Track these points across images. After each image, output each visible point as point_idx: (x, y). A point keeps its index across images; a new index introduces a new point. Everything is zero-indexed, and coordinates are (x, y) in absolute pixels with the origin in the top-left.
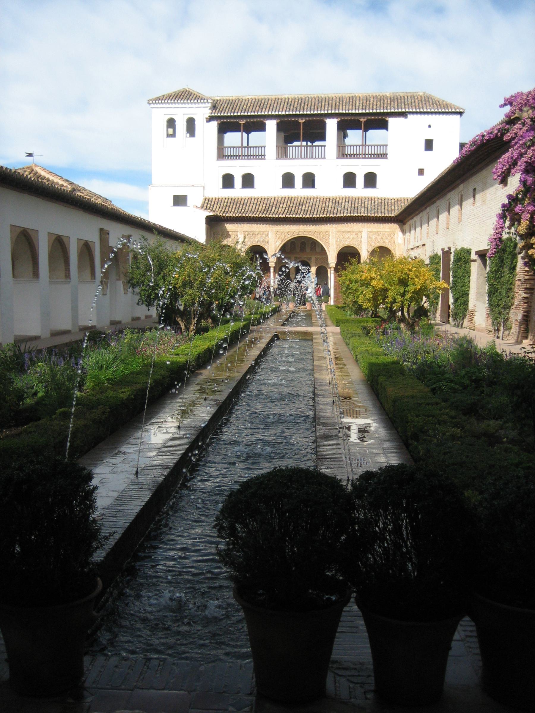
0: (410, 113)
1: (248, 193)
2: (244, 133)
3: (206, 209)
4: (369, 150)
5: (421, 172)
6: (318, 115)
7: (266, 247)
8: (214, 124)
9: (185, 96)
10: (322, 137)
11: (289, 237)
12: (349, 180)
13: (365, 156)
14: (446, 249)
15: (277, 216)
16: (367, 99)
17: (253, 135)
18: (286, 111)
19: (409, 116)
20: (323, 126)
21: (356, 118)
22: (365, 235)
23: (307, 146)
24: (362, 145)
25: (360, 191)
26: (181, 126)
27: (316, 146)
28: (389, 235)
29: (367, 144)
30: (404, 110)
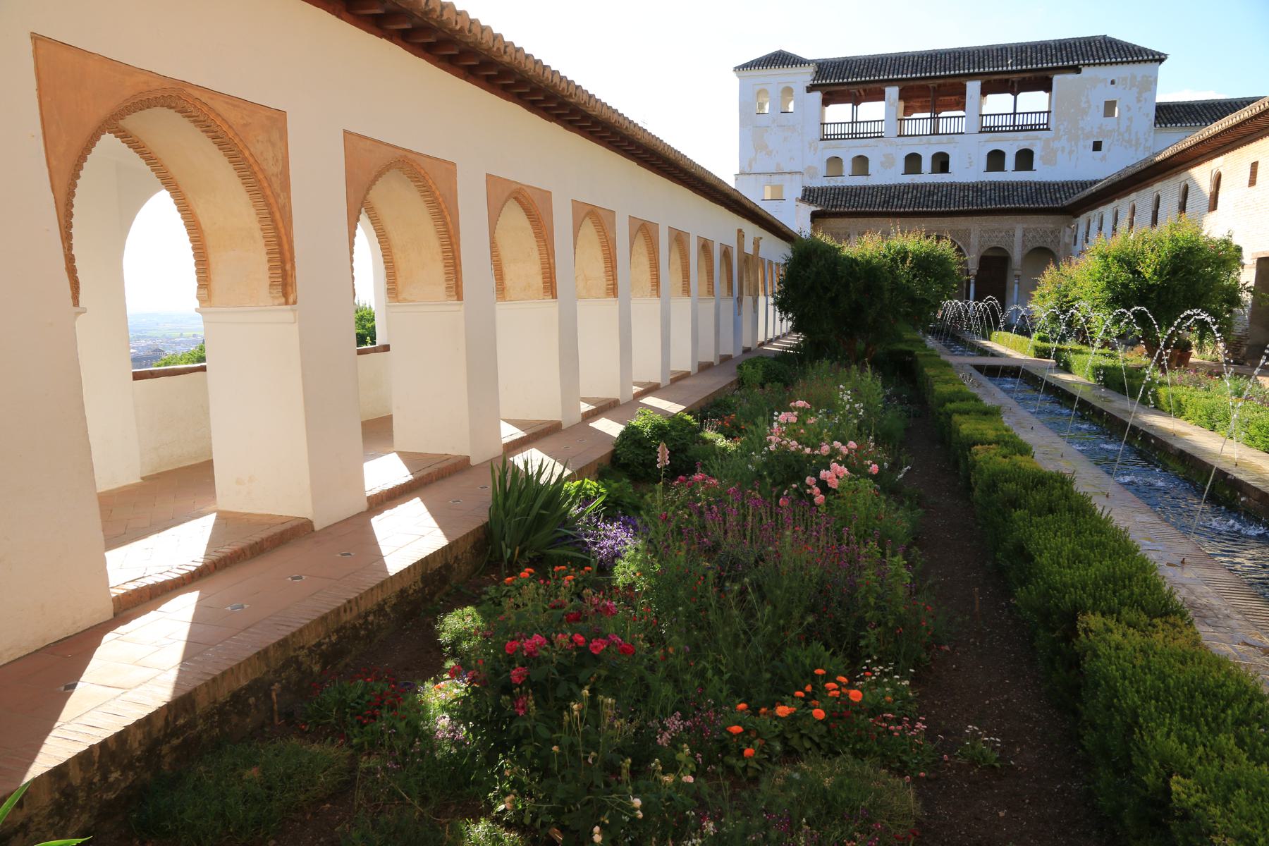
1: (860, 181)
4: (1020, 120)
5: (1097, 146)
8: (817, 96)
9: (780, 60)
12: (996, 160)
17: (864, 107)
20: (962, 93)
22: (1019, 233)
25: (1010, 174)
28: (1052, 232)
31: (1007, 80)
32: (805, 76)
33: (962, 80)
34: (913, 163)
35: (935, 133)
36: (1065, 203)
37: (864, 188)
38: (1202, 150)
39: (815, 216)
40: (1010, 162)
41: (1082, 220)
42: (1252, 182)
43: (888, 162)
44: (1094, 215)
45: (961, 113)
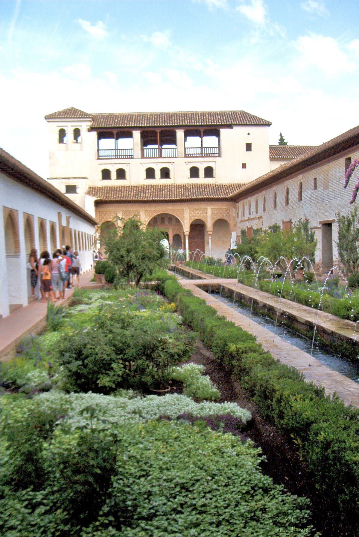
1: (121, 183)
3: (94, 195)
4: (205, 151)
5: (244, 166)
6: (170, 126)
9: (72, 113)
10: (173, 141)
11: (155, 214)
12: (194, 173)
13: (203, 155)
15: (146, 199)
16: (203, 114)
18: (147, 124)
19: (234, 127)
21: (196, 128)
22: (209, 211)
25: (202, 180)
26: (69, 136)
28: (226, 211)
29: (204, 146)
31: (197, 130)
35: (160, 156)
39: (98, 204)
40: (202, 173)
41: (240, 204)
42: (315, 188)
44: (246, 201)
45: (173, 146)
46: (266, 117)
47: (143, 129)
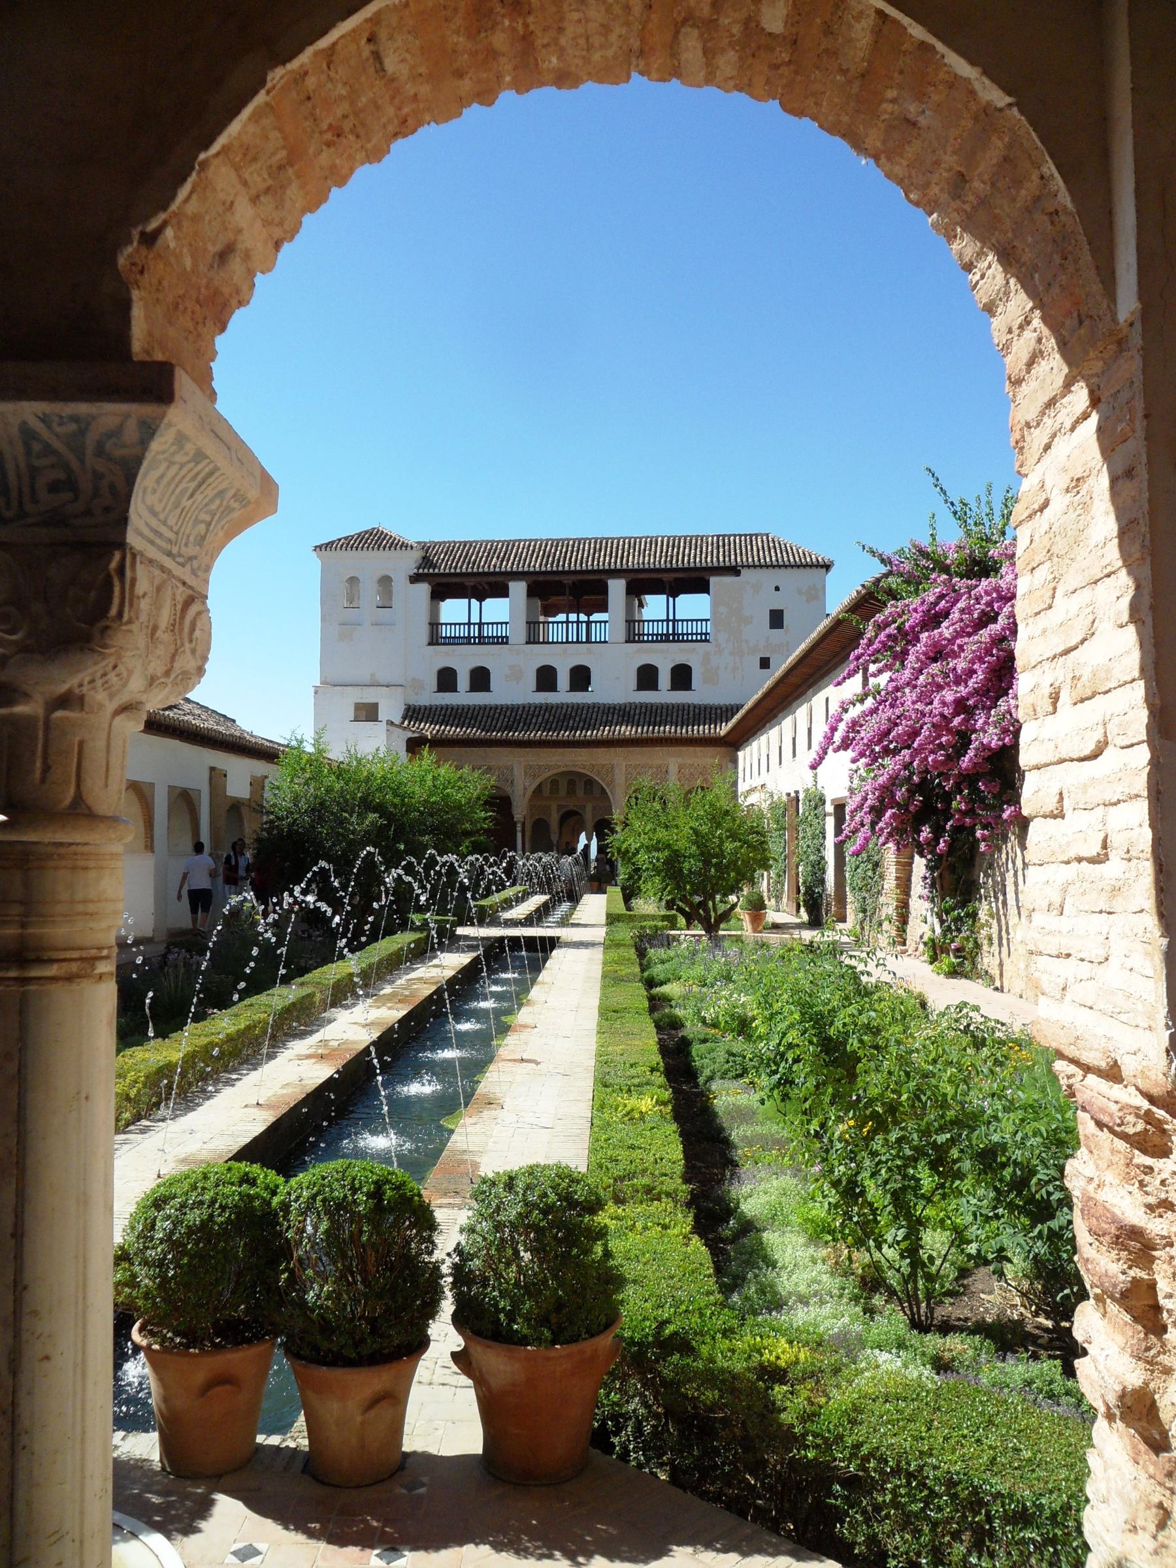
0: (743, 566)
2: (473, 601)
5: (765, 663)
6: (593, 572)
7: (508, 789)
8: (424, 589)
9: (374, 540)
12: (647, 677)
14: (793, 795)
16: (674, 542)
17: (489, 603)
19: (743, 571)
20: (604, 590)
22: (673, 769)
23: (578, 622)
24: (668, 620)
27: (596, 622)
30: (734, 564)
31: (660, 580)
32: (405, 564)
33: (603, 577)
34: (546, 678)
36: (722, 733)
37: (484, 708)
38: (793, 680)
41: (740, 754)
43: (516, 674)
46: (821, 552)
47: (534, 578)
